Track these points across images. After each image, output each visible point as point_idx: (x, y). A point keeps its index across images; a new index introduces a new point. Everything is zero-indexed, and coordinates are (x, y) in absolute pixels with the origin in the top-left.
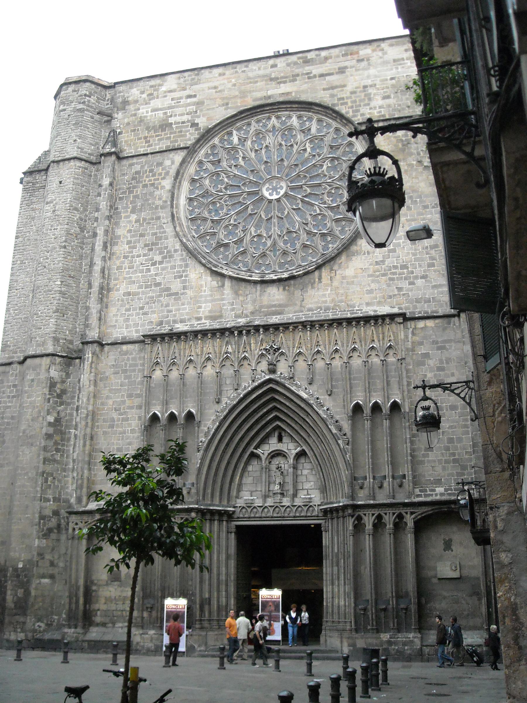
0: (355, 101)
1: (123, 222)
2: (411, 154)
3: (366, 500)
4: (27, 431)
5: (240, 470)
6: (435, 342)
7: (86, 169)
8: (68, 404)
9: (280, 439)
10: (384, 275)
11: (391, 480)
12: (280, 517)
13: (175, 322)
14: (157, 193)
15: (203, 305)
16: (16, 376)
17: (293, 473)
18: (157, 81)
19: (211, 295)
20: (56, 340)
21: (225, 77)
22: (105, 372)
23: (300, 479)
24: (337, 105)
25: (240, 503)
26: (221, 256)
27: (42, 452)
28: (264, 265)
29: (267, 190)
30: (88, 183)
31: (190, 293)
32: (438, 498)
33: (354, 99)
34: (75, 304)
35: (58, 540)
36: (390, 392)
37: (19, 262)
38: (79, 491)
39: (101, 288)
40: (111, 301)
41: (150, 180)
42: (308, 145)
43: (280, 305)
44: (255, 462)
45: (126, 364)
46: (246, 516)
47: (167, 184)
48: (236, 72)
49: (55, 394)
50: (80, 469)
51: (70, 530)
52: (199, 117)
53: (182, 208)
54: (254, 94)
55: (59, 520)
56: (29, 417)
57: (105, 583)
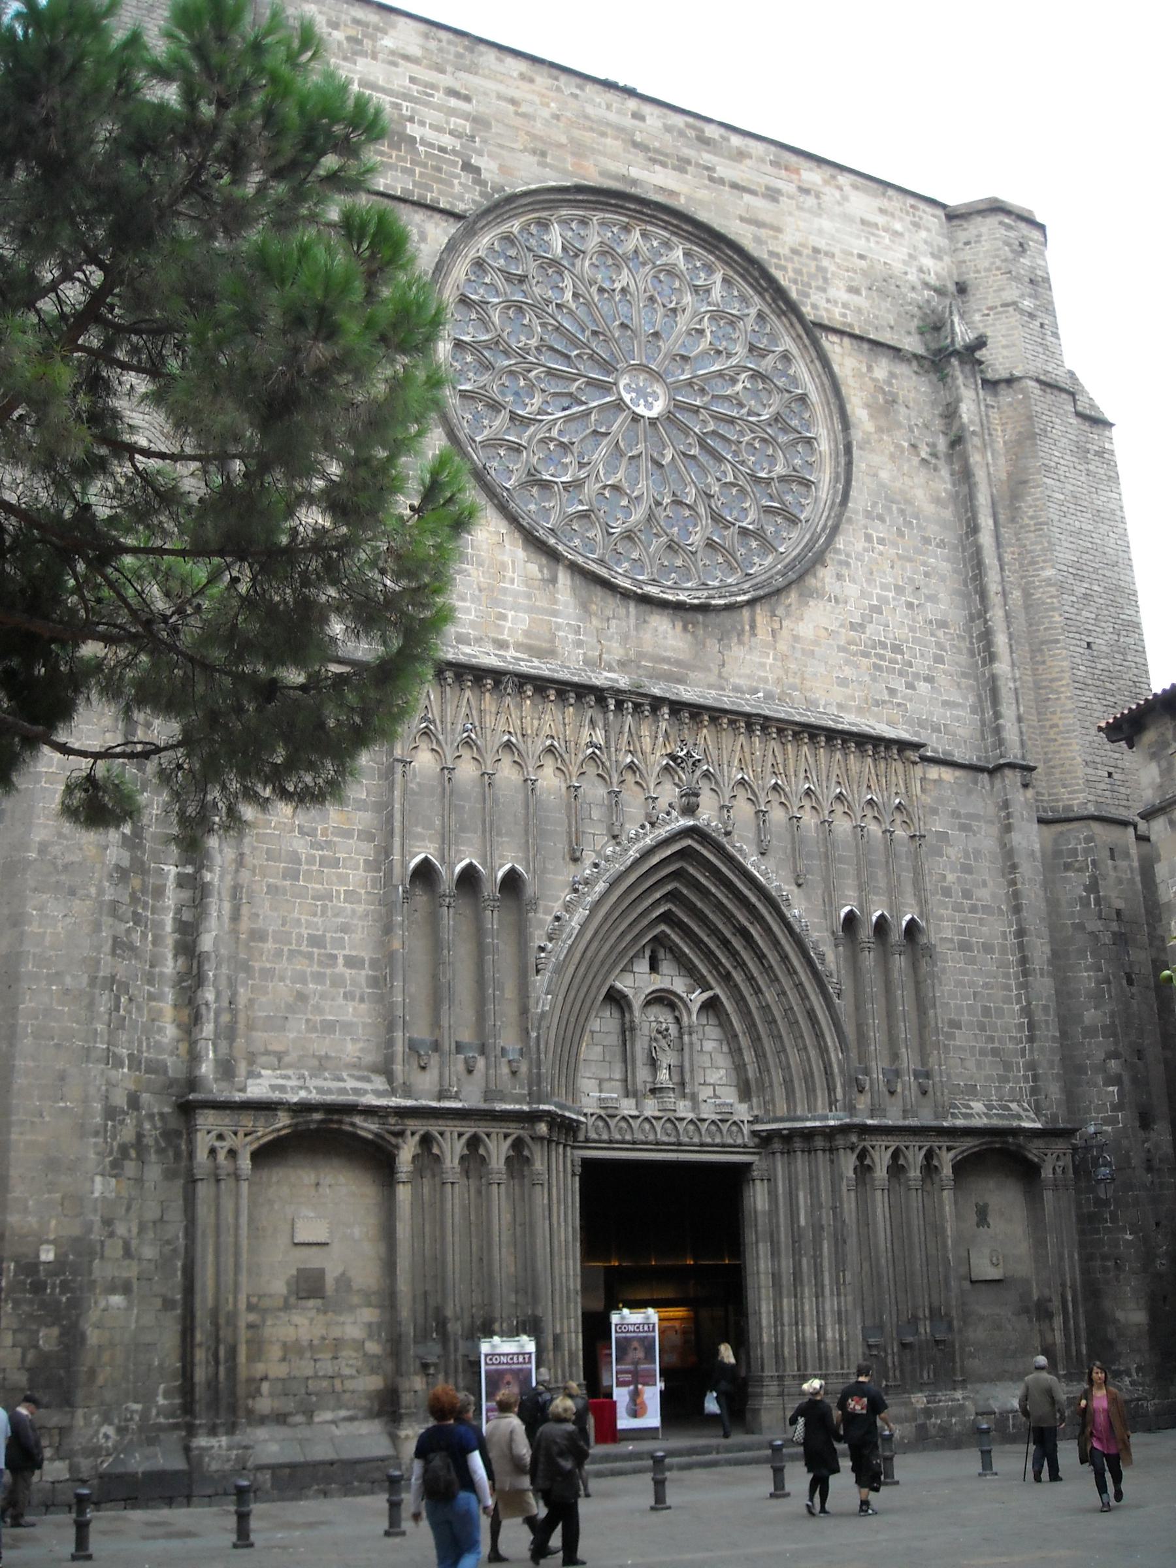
2: (899, 425)
4: (55, 850)
6: (955, 814)
9: (654, 967)
10: (866, 655)
15: (510, 614)
21: (533, 87)
27: (107, 920)
28: (628, 559)
29: (628, 387)
33: (797, 266)
35: (139, 1181)
43: (678, 663)
48: (558, 89)
50: (223, 982)
52: (480, 154)
54: (602, 159)
55: (139, 1124)
57: (280, 1303)
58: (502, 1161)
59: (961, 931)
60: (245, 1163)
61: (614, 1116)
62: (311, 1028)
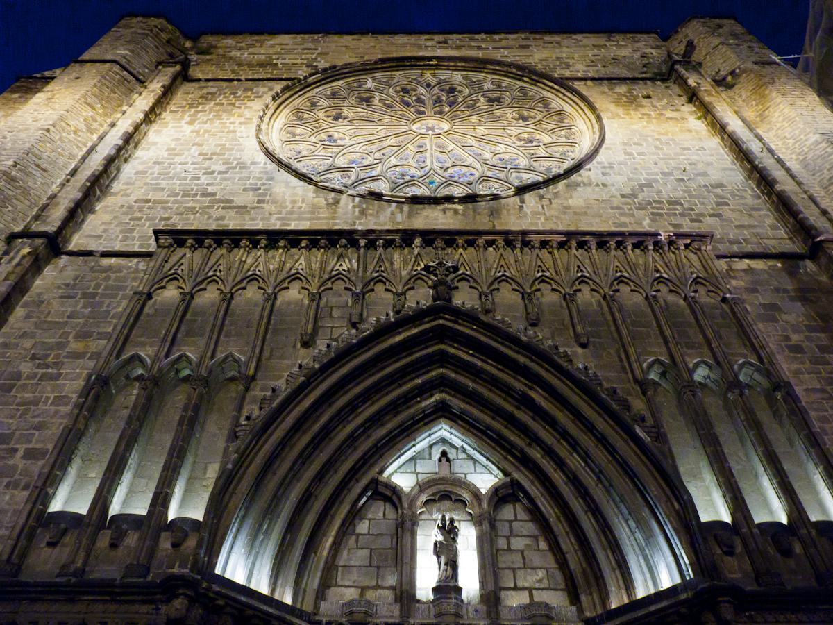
5: (337, 523)
7: (129, 82)
19: (313, 213)
23: (504, 560)
45: (98, 286)
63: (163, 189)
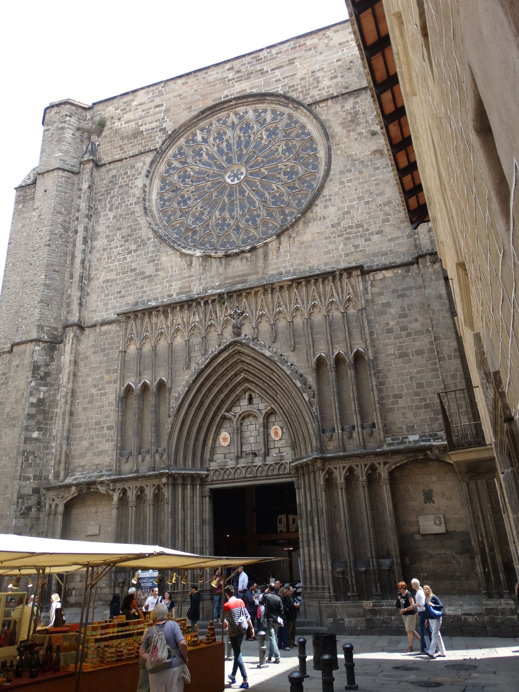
0: (305, 86)
1: (102, 220)
3: (336, 452)
4: (11, 414)
5: (213, 434)
6: (394, 291)
7: (70, 178)
8: (52, 385)
10: (339, 236)
11: (360, 429)
12: (252, 477)
13: (149, 301)
14: (131, 191)
15: (174, 284)
16: (6, 365)
17: (264, 432)
18: (130, 97)
19: (181, 274)
20: (40, 328)
21: (187, 85)
22: (85, 352)
24: (289, 92)
25: (214, 466)
26: (189, 240)
27: (24, 432)
28: (229, 243)
29: (229, 177)
30: (72, 190)
31: (161, 274)
32: (412, 445)
33: (303, 84)
34: (59, 295)
35: (38, 519)
36: (353, 343)
37: (11, 265)
38: (56, 466)
39: (81, 277)
40: (92, 289)
41: (125, 182)
42: (264, 133)
43: (244, 275)
44: (227, 424)
45: (105, 343)
46: (220, 478)
47: (140, 182)
48: (198, 79)
49: (39, 377)
50: (58, 444)
51: (47, 507)
53: (154, 202)
54: (214, 95)
56: (13, 400)
58: (151, 495)
59: (401, 348)
60: (61, 508)
61: (223, 469)
62: (94, 454)
63: (112, 270)
